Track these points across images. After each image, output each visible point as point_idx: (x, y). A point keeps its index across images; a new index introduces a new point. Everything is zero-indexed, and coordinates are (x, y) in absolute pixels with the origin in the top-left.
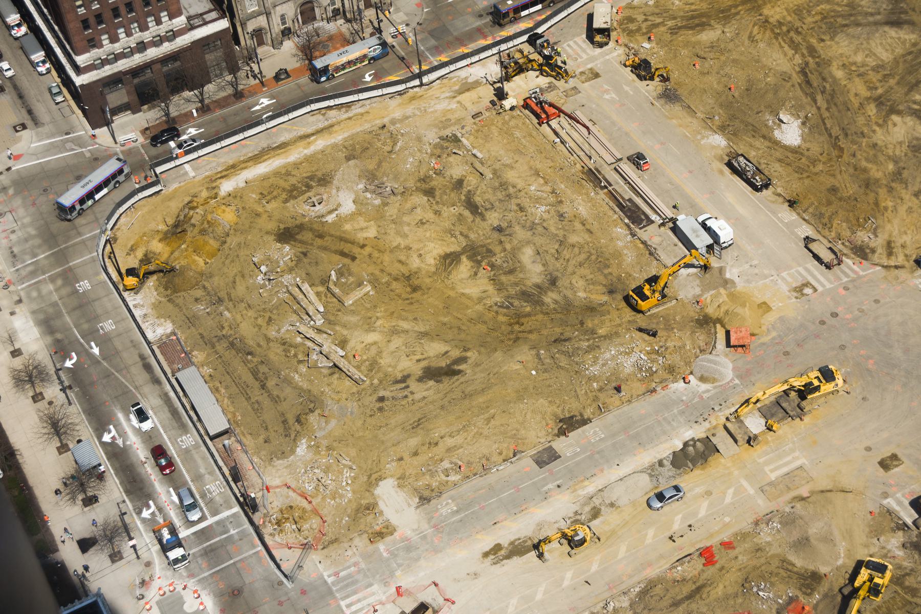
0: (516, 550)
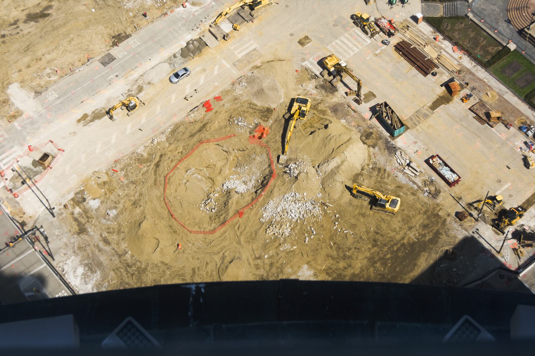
0: (97, 116)
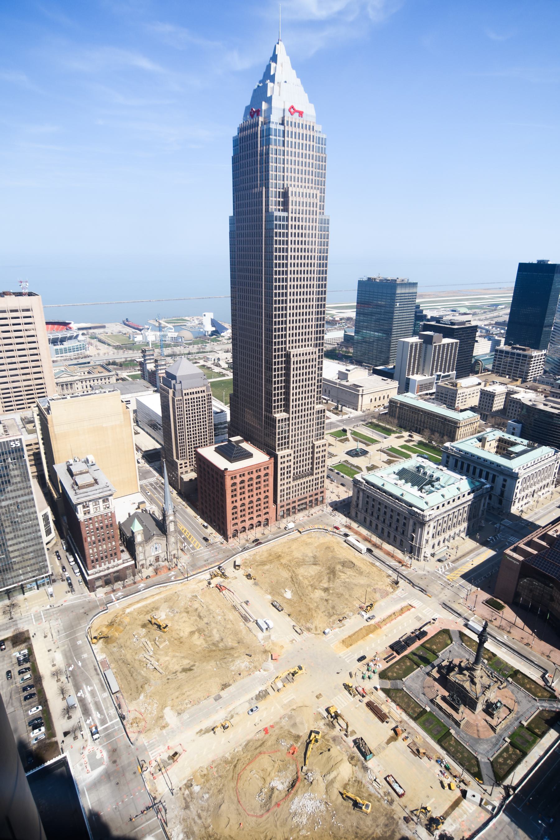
0: (207, 731)
